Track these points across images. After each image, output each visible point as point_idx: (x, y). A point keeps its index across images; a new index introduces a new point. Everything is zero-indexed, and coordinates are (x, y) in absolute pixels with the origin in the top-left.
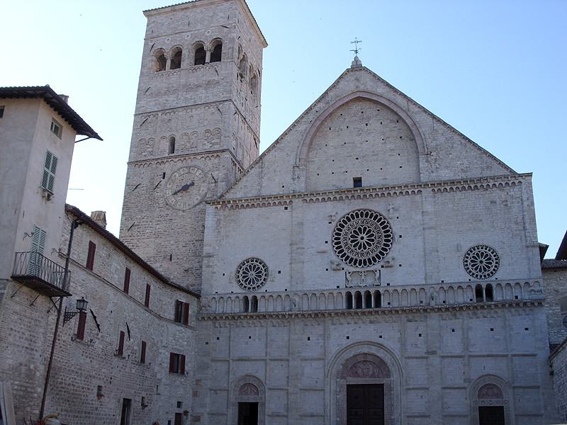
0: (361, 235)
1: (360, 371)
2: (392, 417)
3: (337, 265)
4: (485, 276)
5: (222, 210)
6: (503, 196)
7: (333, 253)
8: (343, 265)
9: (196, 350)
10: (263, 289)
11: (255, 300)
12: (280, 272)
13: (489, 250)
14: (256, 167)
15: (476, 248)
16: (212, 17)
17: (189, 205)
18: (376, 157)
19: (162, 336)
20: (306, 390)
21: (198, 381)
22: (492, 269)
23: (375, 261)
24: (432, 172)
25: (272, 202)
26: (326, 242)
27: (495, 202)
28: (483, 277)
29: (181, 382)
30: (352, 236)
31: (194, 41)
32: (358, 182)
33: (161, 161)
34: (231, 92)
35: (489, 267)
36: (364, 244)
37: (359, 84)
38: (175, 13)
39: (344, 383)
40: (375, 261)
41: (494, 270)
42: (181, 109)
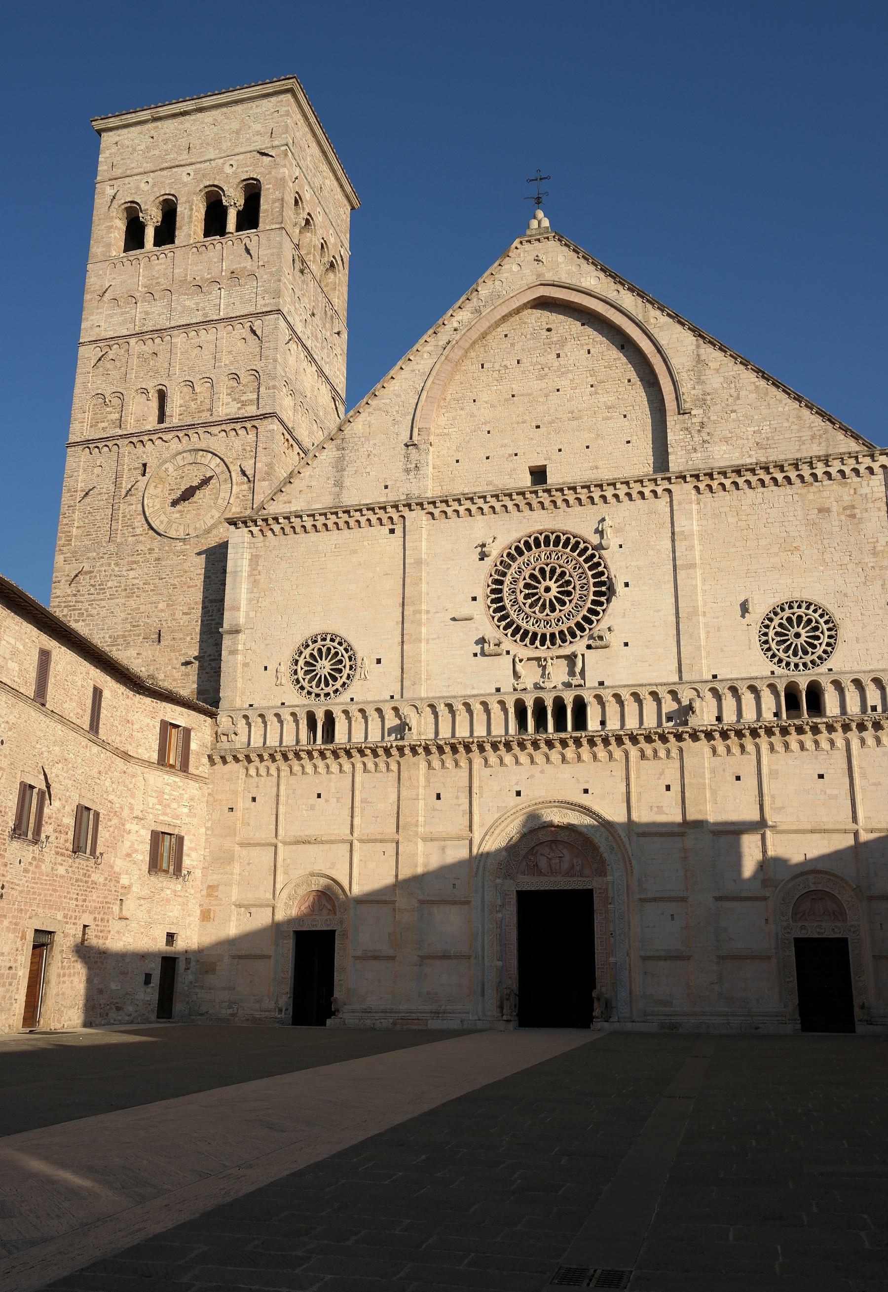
1: (543, 863)
2: (612, 960)
3: (498, 645)
4: (805, 665)
6: (846, 498)
7: (487, 621)
8: (508, 644)
9: (209, 825)
10: (345, 697)
12: (379, 661)
13: (815, 611)
14: (330, 447)
15: (786, 607)
16: (238, 132)
17: (195, 529)
18: (575, 423)
20: (431, 902)
21: (211, 888)
22: (819, 651)
23: (574, 635)
24: (695, 450)
26: (474, 599)
27: (828, 510)
28: (801, 667)
29: (175, 891)
30: (527, 586)
31: (202, 186)
32: (539, 474)
33: (137, 438)
34: (277, 294)
35: (814, 647)
36: (550, 600)
37: (540, 268)
38: (159, 124)
39: (512, 887)
40: (574, 635)
41: (825, 652)
42: (176, 332)
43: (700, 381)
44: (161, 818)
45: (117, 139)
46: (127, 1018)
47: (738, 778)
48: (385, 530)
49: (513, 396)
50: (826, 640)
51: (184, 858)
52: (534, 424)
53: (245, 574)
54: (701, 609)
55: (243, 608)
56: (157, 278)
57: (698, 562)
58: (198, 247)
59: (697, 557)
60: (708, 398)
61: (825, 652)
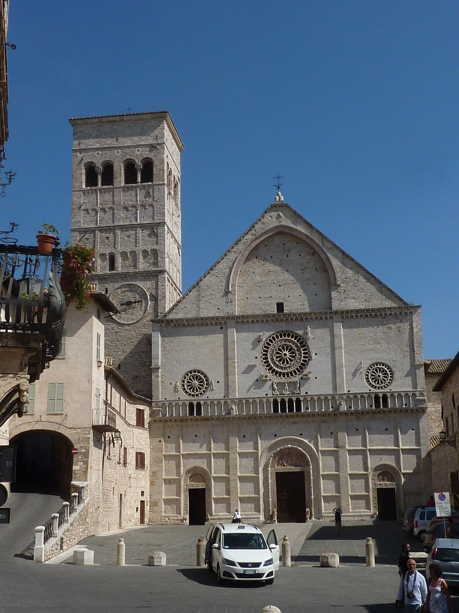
0: (284, 352)
5: (166, 328)
10: (204, 397)
11: (199, 405)
14: (194, 290)
19: (130, 440)
22: (387, 382)
25: (209, 323)
26: (256, 358)
32: (280, 306)
34: (163, 214)
43: (344, 272)
44: (138, 447)
45: (82, 129)
46: (132, 524)
47: (357, 430)
48: (219, 327)
49: (269, 272)
50: (389, 378)
51: (145, 461)
52: (278, 285)
53: (160, 344)
54: (344, 365)
55: (160, 359)
56: (106, 201)
57: (343, 346)
58: (125, 189)
59: (343, 344)
60: (347, 279)
61: (389, 383)
